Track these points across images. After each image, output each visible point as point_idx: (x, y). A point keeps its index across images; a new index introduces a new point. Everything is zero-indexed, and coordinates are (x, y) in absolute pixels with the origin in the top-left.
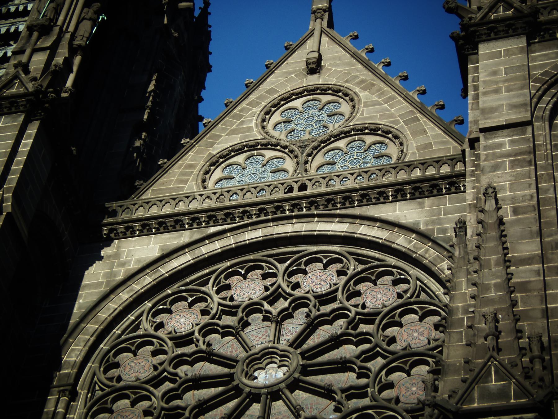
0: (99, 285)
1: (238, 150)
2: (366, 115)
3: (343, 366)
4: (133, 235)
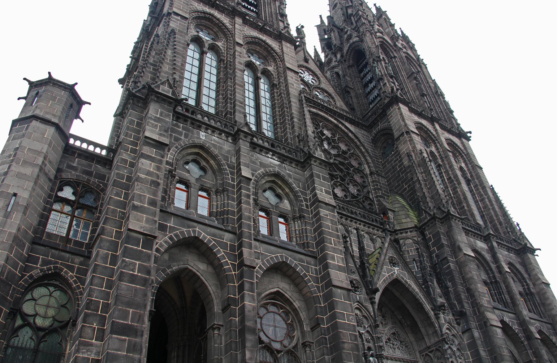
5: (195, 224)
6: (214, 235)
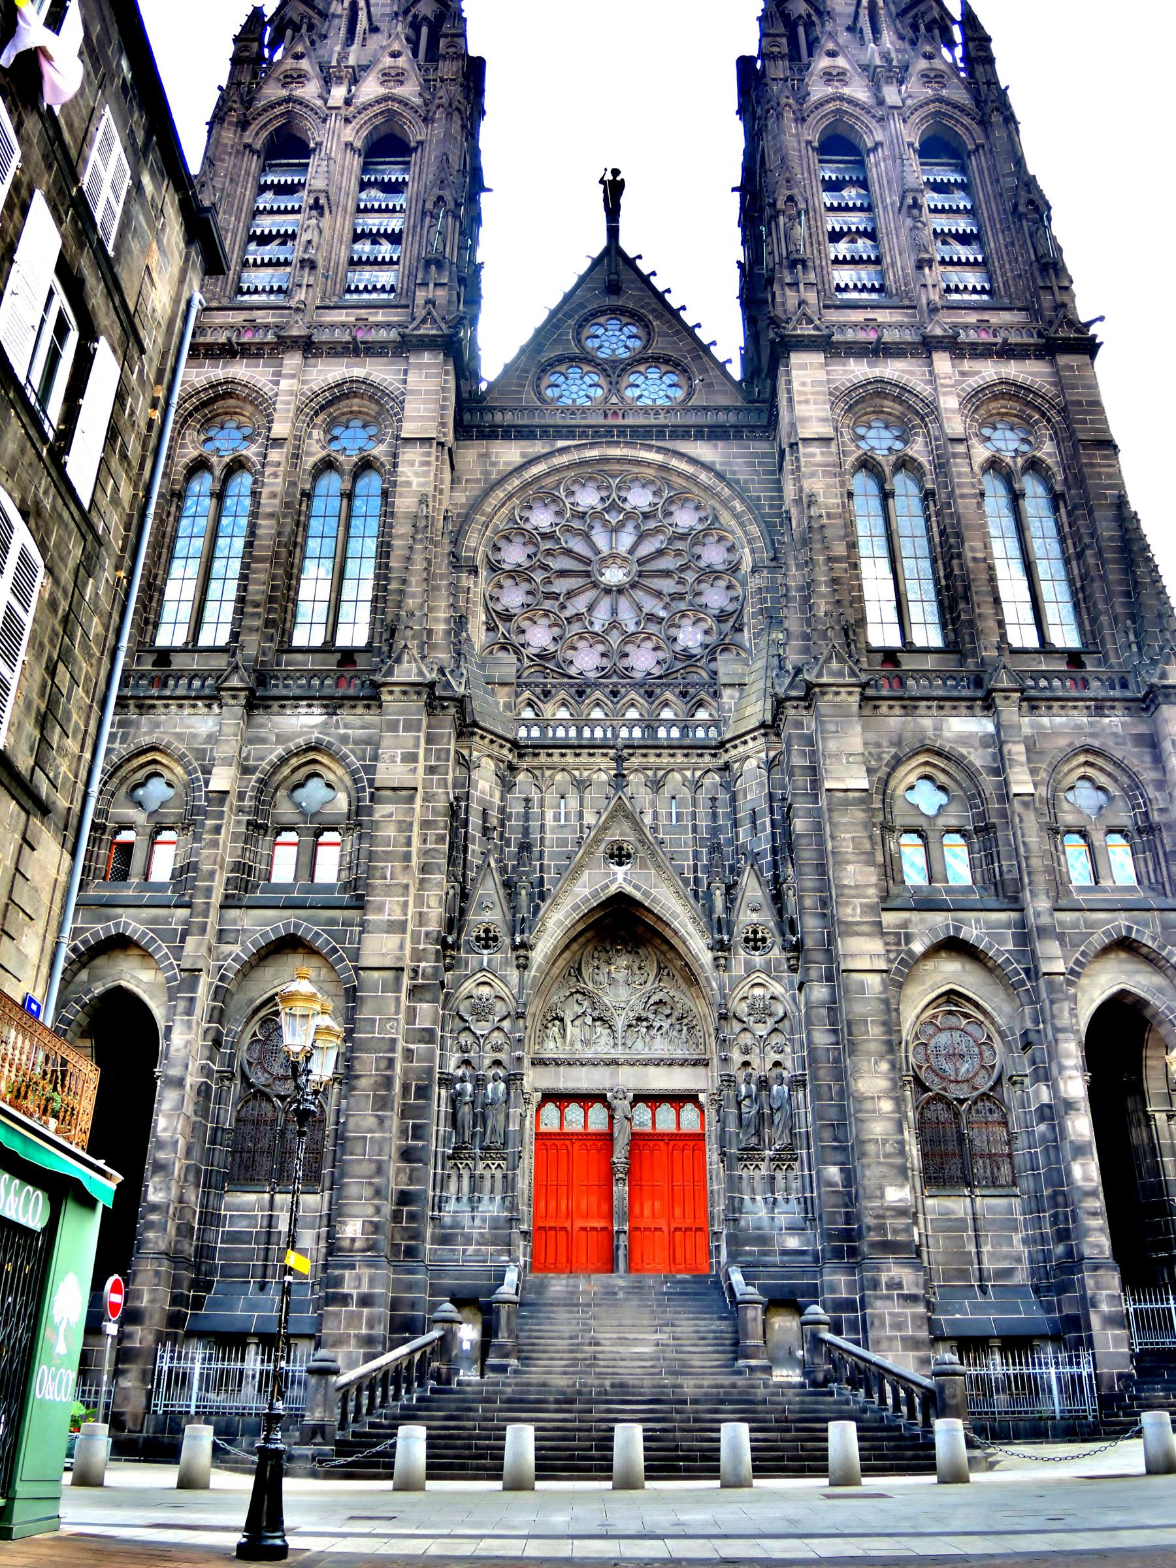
0: (477, 481)
1: (561, 360)
2: (659, 346)
3: (667, 574)
4: (496, 438)
5: (120, 911)
6: (155, 921)
